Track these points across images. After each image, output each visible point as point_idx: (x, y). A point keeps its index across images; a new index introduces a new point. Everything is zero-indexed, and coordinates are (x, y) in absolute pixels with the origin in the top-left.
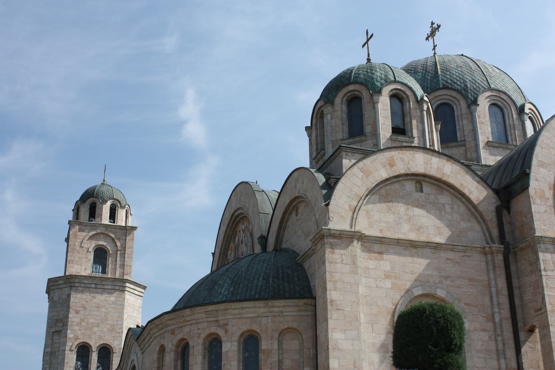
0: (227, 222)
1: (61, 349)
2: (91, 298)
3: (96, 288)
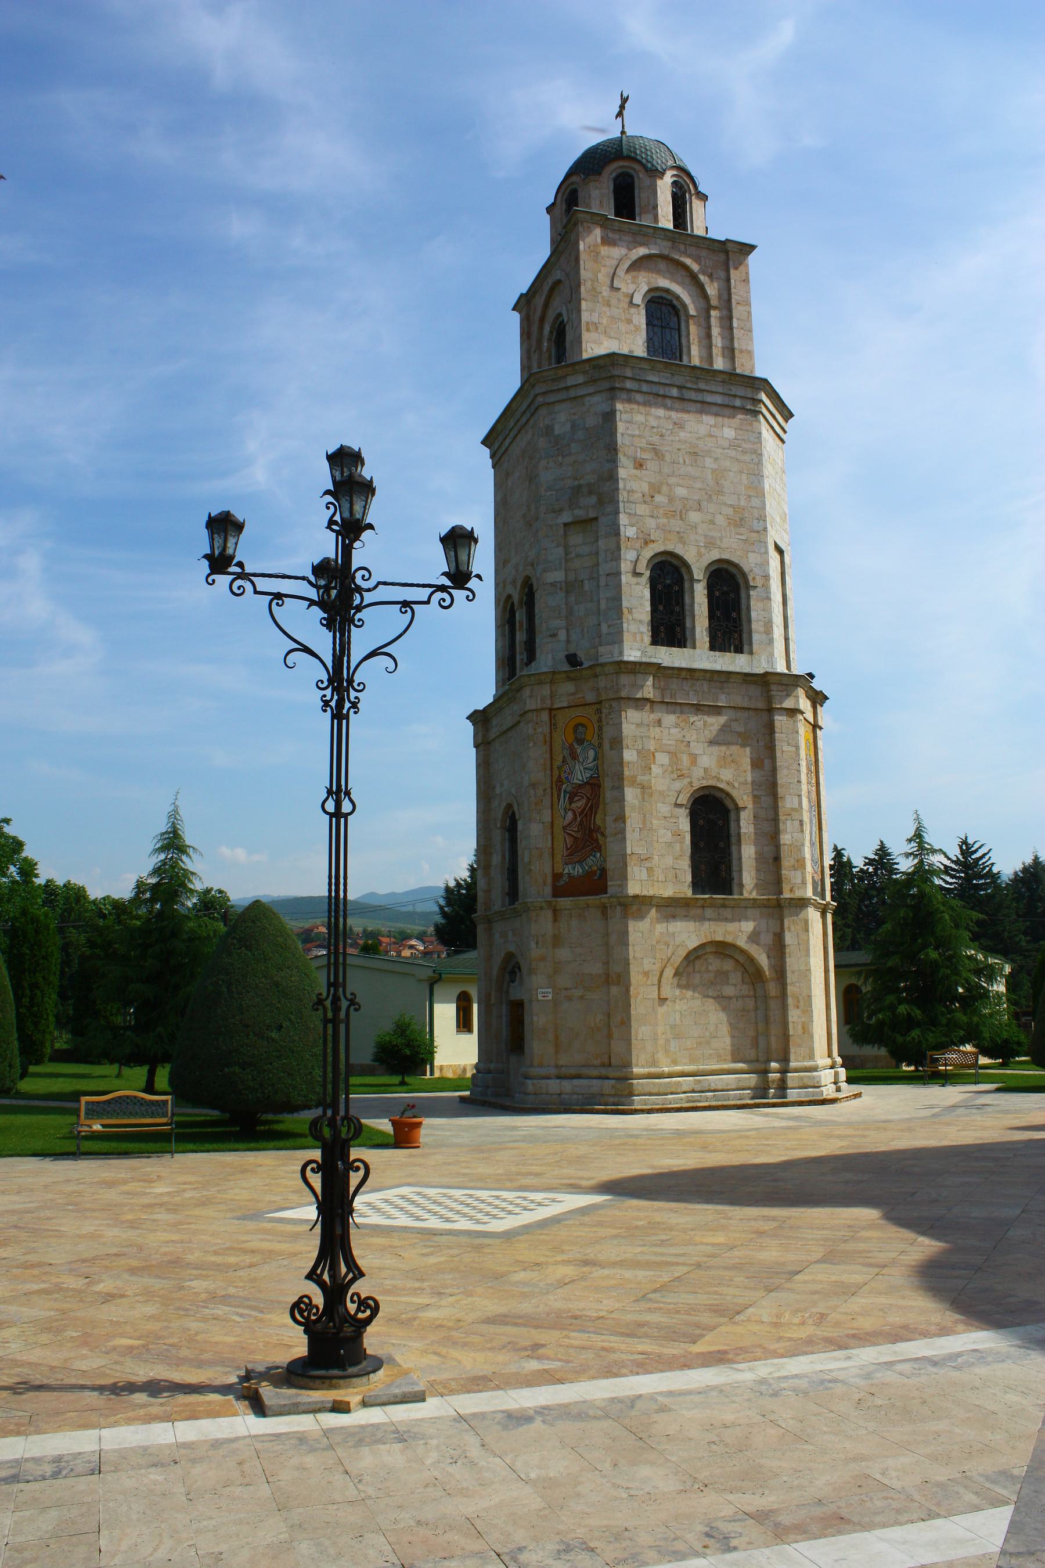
1: (604, 568)
2: (671, 427)
3: (682, 399)
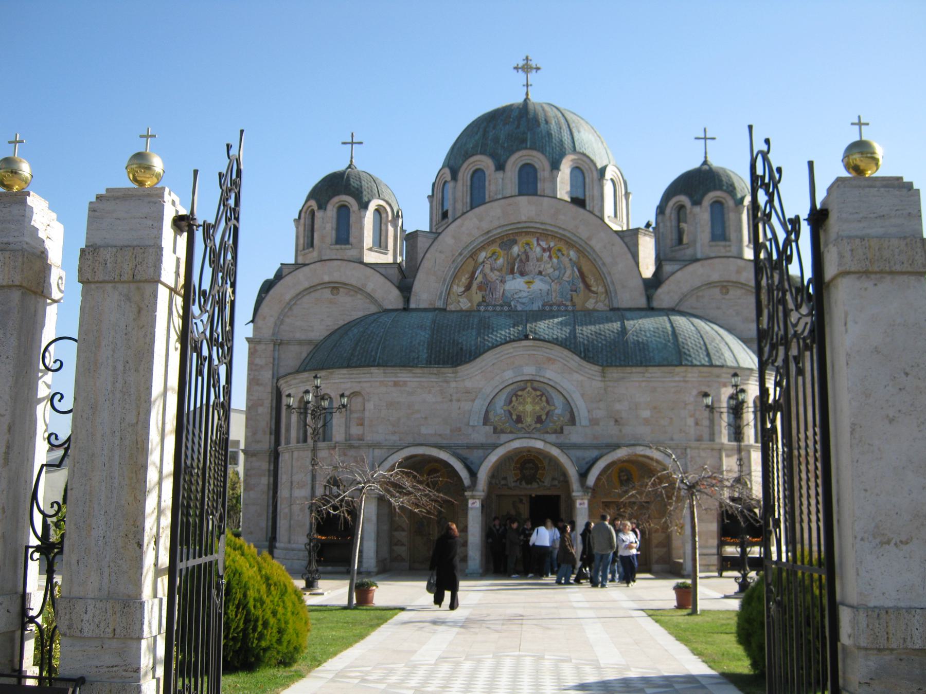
0: (496, 223)
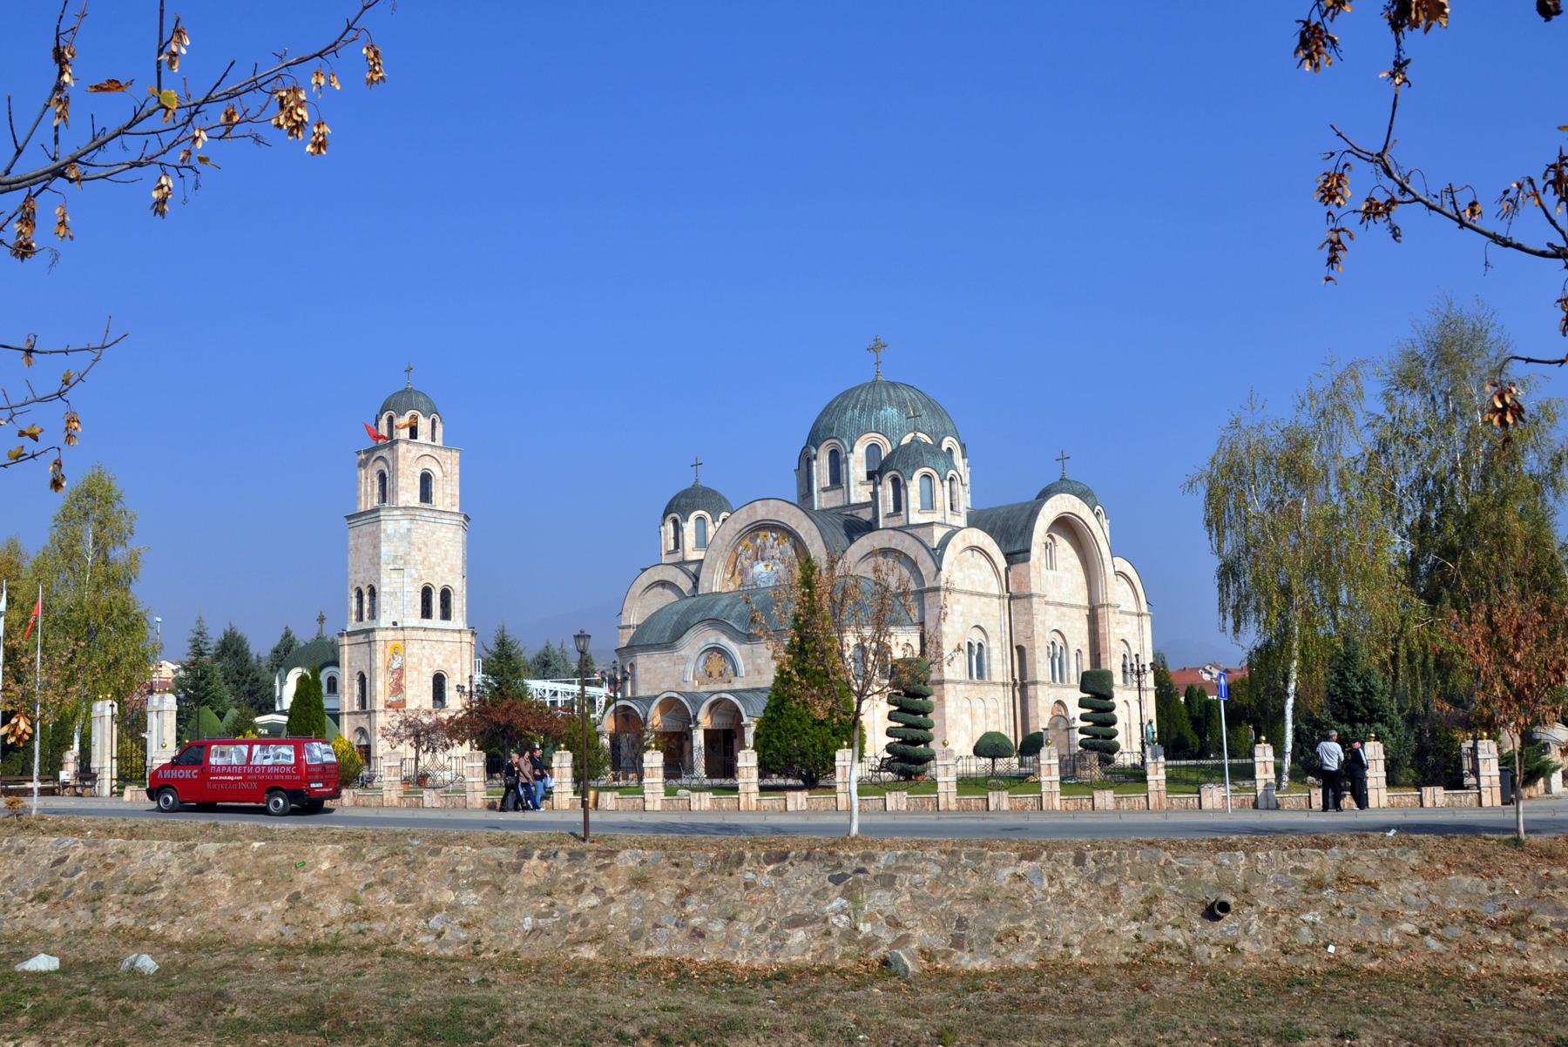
0: (745, 524)
